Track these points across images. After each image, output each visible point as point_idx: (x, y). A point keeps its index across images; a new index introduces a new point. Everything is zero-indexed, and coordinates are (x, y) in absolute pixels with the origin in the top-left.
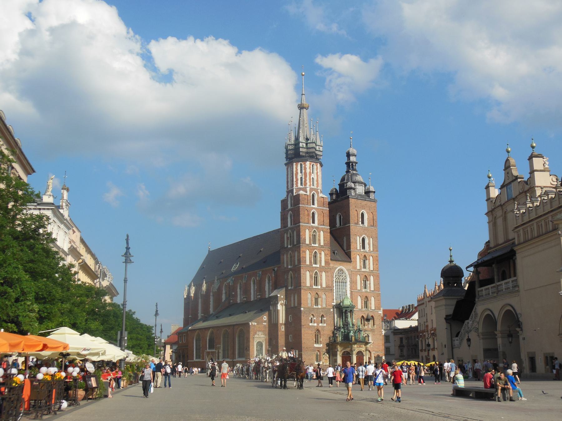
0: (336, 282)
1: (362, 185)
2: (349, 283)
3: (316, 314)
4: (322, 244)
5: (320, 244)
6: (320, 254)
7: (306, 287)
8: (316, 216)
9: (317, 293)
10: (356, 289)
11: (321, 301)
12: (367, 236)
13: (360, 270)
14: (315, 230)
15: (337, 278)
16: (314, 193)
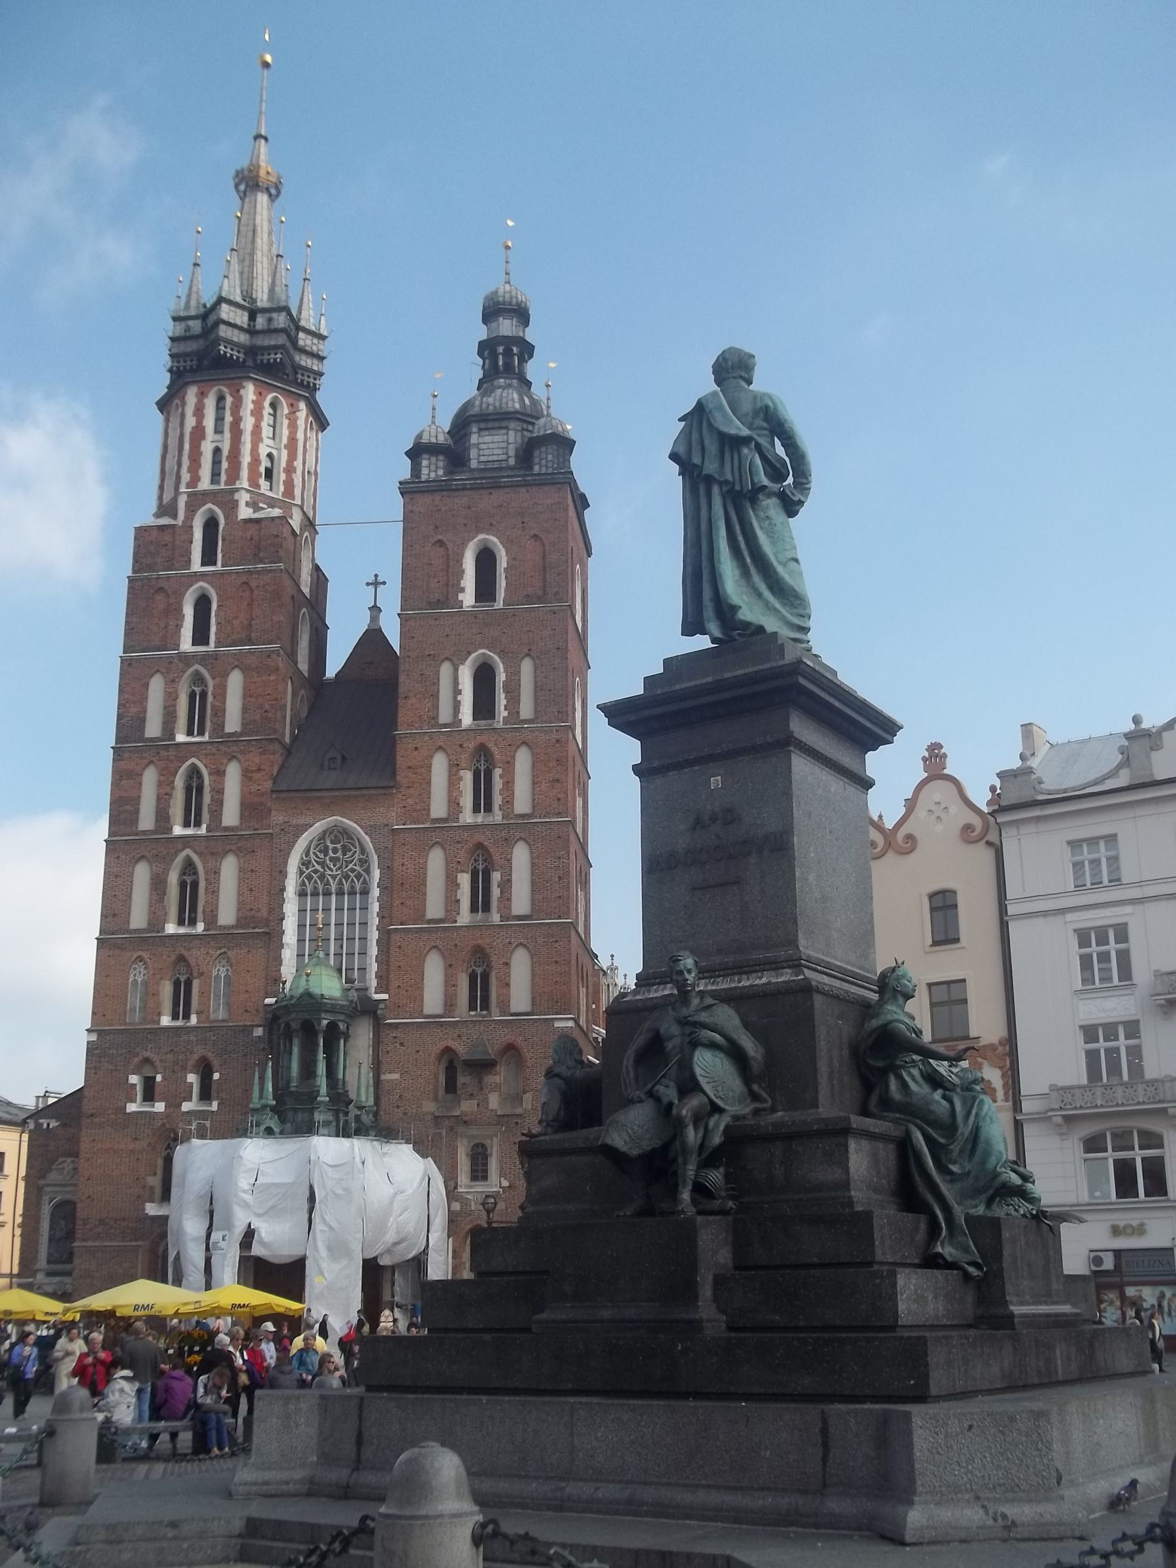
0: (302, 894)
1: (504, 424)
2: (376, 892)
3: (171, 1056)
4: (233, 723)
5: (219, 726)
6: (219, 773)
7: (129, 931)
8: (214, 606)
9: (182, 959)
10: (420, 915)
11: (202, 993)
12: (502, 653)
13: (445, 820)
14: (197, 673)
15: (309, 878)
16: (210, 510)
